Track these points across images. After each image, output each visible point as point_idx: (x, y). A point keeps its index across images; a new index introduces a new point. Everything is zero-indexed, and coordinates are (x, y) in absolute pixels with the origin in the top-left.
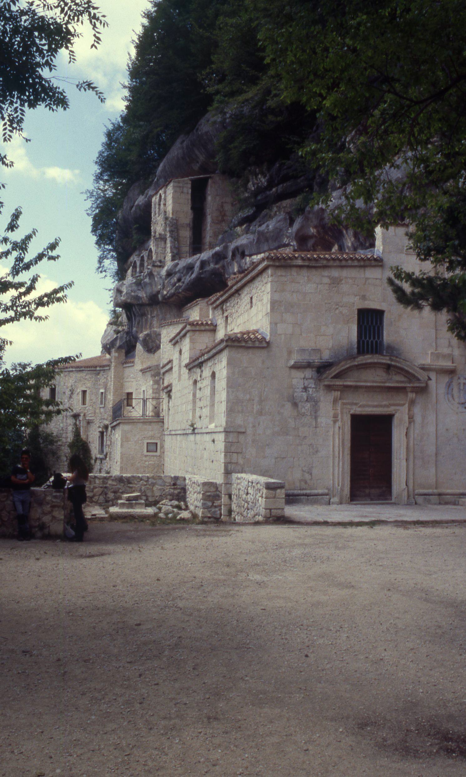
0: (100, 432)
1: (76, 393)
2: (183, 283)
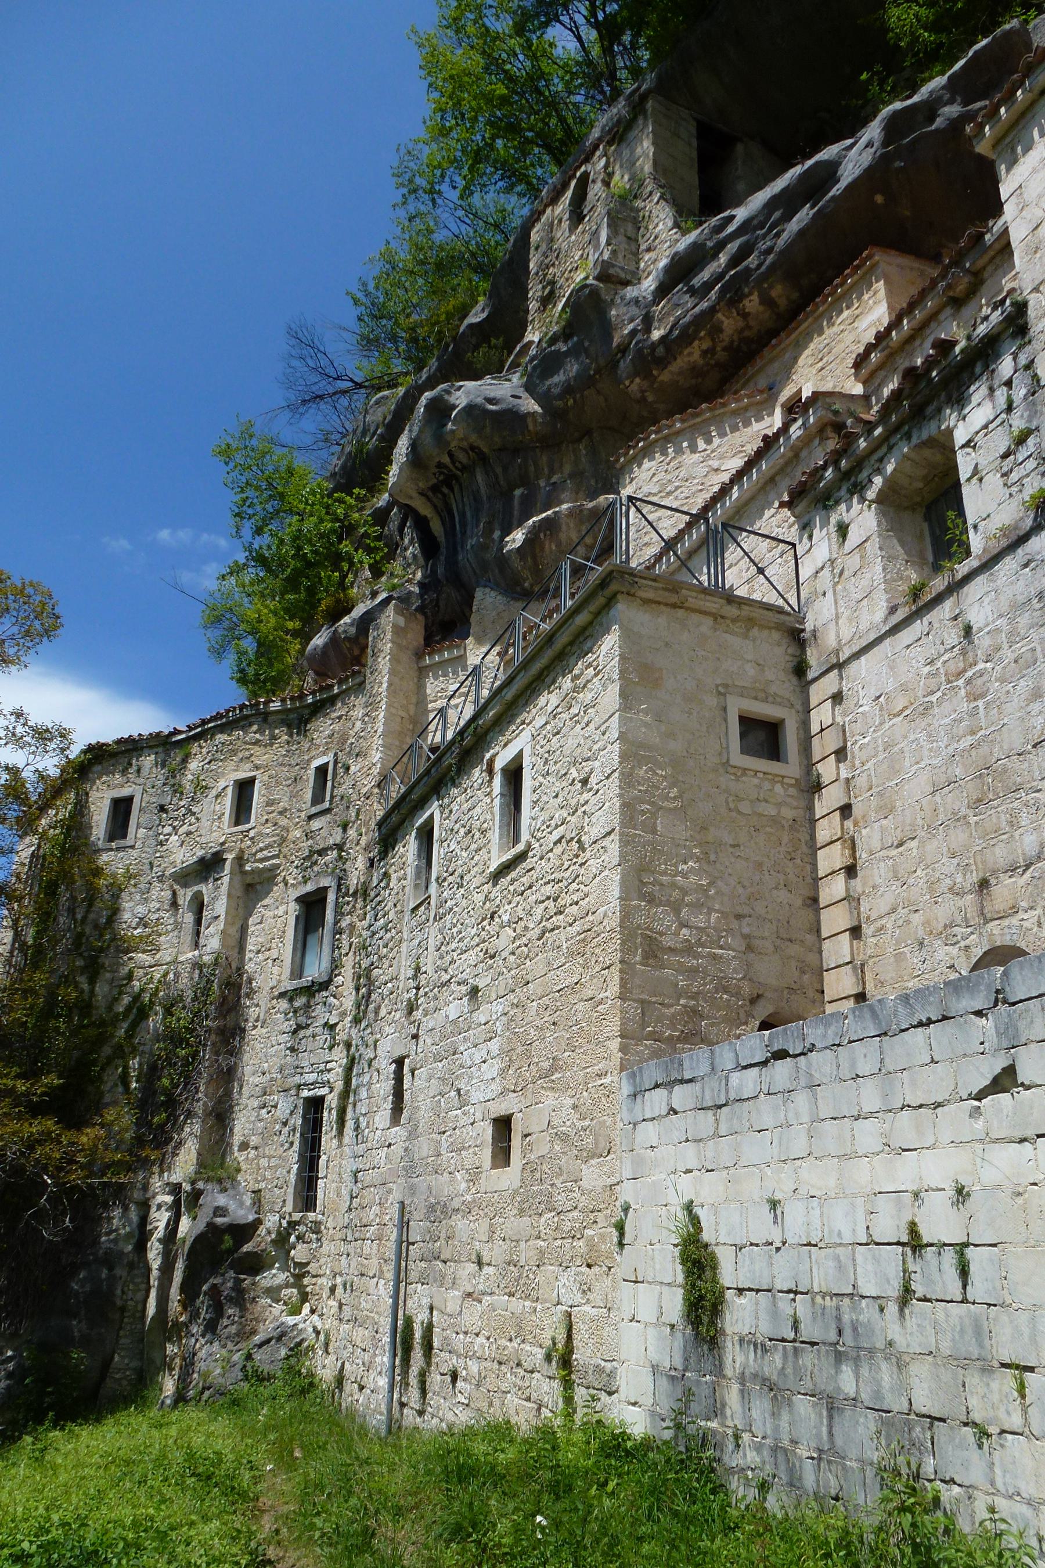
0: (299, 900)
1: (214, 792)
2: (769, 251)
